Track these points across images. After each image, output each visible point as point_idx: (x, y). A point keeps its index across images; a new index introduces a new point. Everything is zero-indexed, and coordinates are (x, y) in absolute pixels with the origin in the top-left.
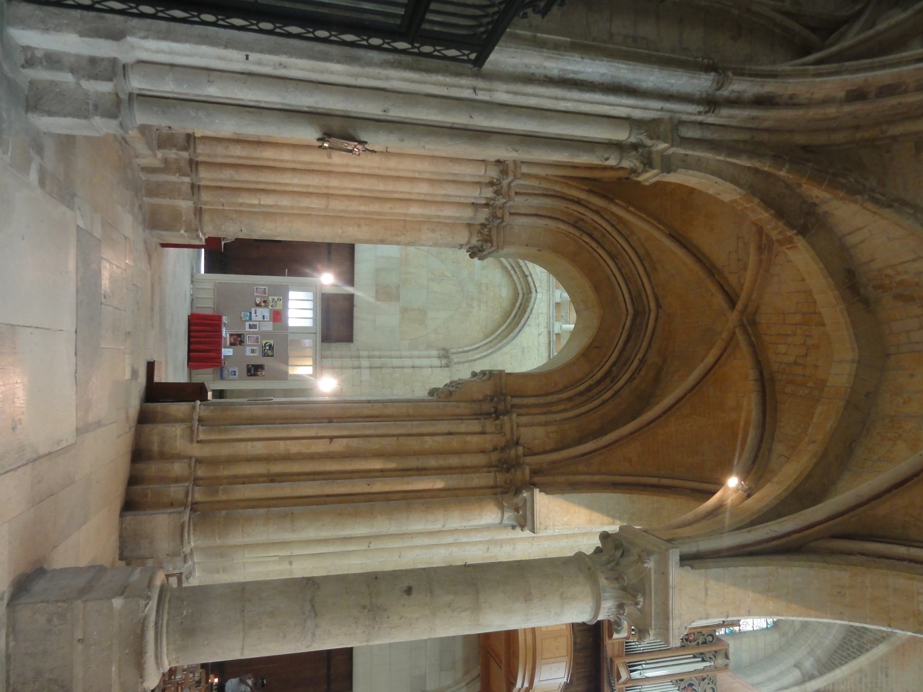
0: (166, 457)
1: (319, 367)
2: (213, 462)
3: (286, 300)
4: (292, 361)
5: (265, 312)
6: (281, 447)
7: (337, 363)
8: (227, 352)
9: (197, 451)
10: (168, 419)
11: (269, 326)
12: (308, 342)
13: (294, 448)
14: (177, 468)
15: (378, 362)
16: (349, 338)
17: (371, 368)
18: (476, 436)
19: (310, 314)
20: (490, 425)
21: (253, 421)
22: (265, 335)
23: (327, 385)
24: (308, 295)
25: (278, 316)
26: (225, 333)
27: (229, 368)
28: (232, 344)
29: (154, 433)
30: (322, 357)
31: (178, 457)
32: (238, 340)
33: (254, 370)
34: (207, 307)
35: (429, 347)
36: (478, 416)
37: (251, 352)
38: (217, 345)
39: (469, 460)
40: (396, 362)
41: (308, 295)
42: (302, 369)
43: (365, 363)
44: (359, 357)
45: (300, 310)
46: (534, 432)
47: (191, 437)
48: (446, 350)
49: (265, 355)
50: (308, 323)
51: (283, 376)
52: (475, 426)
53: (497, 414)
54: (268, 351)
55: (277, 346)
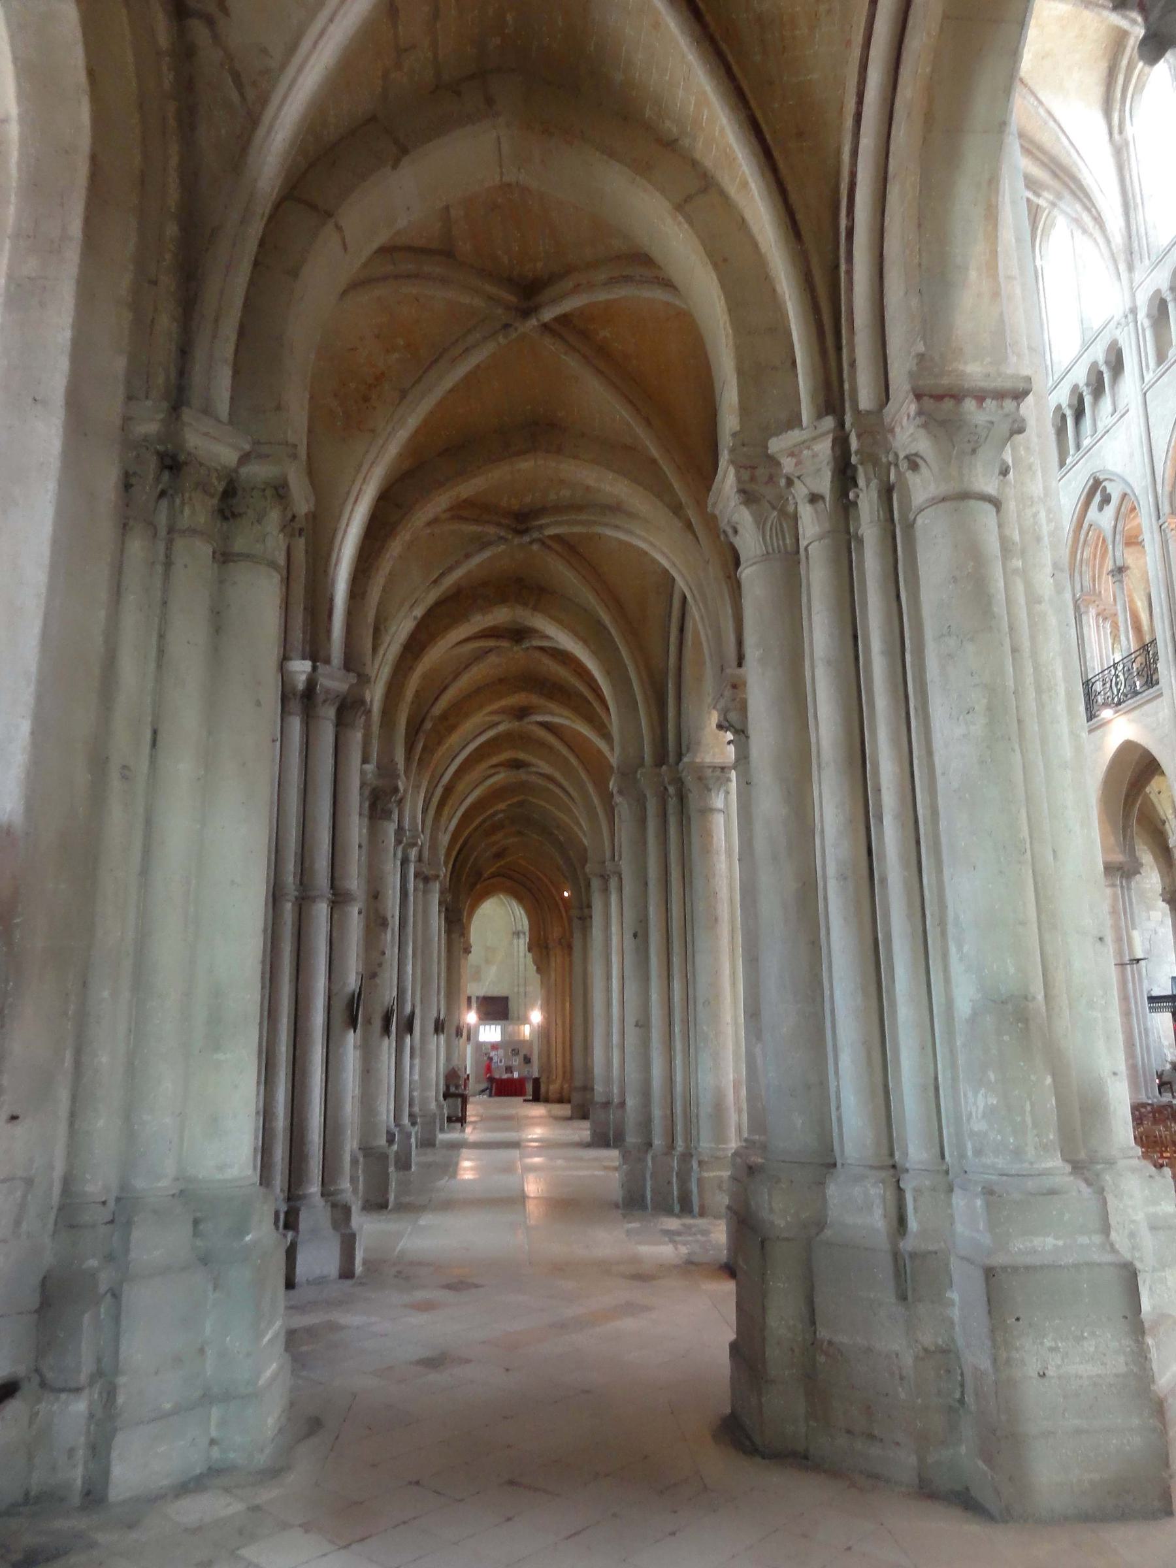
1: (525, 1020)
2: (564, 1073)
3: (484, 1043)
4: (522, 1038)
6: (560, 1046)
8: (516, 1075)
9: (559, 1081)
10: (547, 1092)
11: (501, 1052)
12: (510, 1028)
13: (560, 1040)
14: (566, 1086)
17: (525, 985)
18: (557, 960)
19: (493, 1027)
21: (549, 1056)
22: (506, 1054)
23: (536, 1016)
24: (482, 1028)
25: (495, 1046)
26: (505, 1076)
27: (525, 1074)
29: (552, 1095)
30: (519, 1019)
31: (562, 1088)
32: (509, 1069)
33: (527, 1060)
35: (511, 944)
37: (516, 1062)
38: (511, 1081)
40: (522, 968)
41: (482, 1028)
42: (526, 1031)
45: (491, 1034)
46: (556, 933)
49: (518, 1054)
50: (499, 1028)
51: (531, 1043)
52: (553, 959)
54: (515, 1052)
55: (512, 1046)
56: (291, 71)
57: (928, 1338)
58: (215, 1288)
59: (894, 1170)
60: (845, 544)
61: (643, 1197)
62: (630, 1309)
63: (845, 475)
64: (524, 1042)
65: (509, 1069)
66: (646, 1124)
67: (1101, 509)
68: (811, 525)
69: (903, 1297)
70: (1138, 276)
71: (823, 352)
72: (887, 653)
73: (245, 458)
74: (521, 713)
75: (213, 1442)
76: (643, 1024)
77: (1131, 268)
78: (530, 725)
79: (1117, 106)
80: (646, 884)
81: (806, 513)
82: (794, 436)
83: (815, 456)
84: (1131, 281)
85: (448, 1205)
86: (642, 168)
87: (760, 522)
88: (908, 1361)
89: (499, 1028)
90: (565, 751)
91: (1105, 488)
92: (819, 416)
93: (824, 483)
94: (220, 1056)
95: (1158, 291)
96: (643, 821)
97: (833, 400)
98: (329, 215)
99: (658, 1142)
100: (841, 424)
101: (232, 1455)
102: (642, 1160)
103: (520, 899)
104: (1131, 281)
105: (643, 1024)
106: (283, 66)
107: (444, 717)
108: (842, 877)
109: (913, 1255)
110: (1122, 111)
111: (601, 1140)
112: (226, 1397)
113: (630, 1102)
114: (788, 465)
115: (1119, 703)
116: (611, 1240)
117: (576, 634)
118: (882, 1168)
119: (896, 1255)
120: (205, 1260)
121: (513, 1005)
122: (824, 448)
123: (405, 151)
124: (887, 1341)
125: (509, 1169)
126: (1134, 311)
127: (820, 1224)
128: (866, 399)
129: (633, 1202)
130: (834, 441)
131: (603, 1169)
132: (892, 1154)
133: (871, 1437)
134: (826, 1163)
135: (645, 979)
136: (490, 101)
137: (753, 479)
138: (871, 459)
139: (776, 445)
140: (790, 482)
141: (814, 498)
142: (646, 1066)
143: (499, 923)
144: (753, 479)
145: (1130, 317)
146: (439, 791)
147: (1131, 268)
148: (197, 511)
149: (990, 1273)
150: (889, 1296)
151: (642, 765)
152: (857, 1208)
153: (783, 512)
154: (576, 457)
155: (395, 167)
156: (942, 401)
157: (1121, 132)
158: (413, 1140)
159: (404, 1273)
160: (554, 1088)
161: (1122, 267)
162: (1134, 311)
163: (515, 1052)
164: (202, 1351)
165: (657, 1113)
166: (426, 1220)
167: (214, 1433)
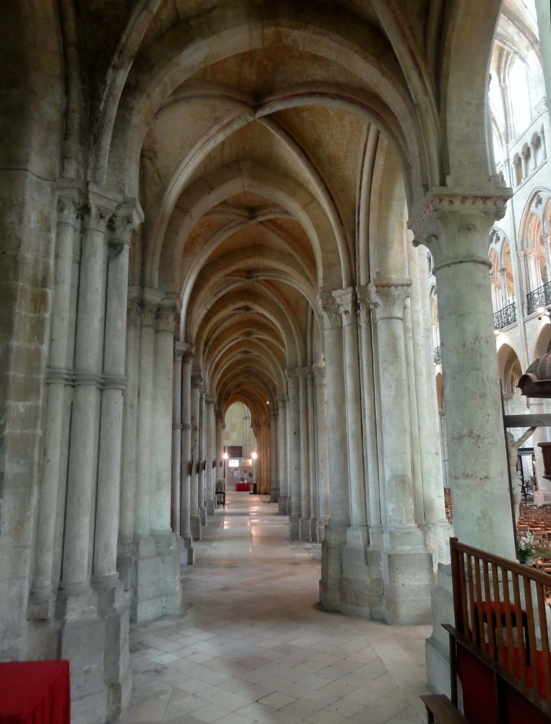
0: (266, 489)
1: (249, 457)
2: (267, 481)
3: (231, 468)
5: (236, 473)
6: (265, 469)
7: (248, 451)
8: (246, 482)
11: (239, 471)
12: (243, 461)
13: (265, 466)
15: (248, 439)
16: (240, 448)
17: (249, 441)
19: (235, 460)
20: (262, 428)
21: (260, 474)
22: (241, 473)
23: (255, 456)
24: (230, 461)
25: (236, 469)
26: (241, 482)
28: (244, 481)
29: (262, 491)
30: (247, 457)
32: (243, 479)
33: (251, 475)
34: (234, 487)
35: (243, 423)
36: (260, 429)
37: (246, 476)
38: (244, 484)
39: (268, 433)
40: (248, 433)
41: (230, 461)
42: (250, 462)
43: (248, 443)
44: (246, 445)
45: (234, 463)
46: (263, 418)
47: (263, 485)
48: (244, 418)
50: (238, 461)
51: (252, 467)
53: (260, 426)
54: (245, 471)
55: (244, 469)
56: (177, 174)
57: (374, 576)
58: (163, 562)
59: (366, 526)
60: (356, 326)
61: (298, 535)
62: (291, 574)
63: (356, 306)
64: (249, 467)
65: (243, 479)
66: (299, 508)
67: (496, 243)
68: (346, 321)
69: (367, 564)
70: (510, 145)
71: (350, 262)
72: (368, 365)
73: (163, 299)
74: (249, 334)
75: (164, 607)
76: (298, 469)
77: (507, 142)
78: (253, 337)
79: (503, 70)
80: (299, 413)
81: (344, 316)
82: (340, 292)
83: (346, 299)
84: (507, 147)
85: (221, 539)
86: (292, 194)
87: (330, 317)
88: (368, 583)
89: (238, 461)
90: (266, 348)
91: (497, 234)
92: (348, 286)
93: (349, 308)
94: (161, 492)
95: (517, 154)
96: (297, 388)
97: (353, 282)
98: (188, 212)
99: (304, 514)
100: (355, 290)
101: (169, 611)
102: (297, 521)
103: (246, 404)
104: (507, 147)
105: (298, 469)
106: (174, 172)
107: (217, 339)
108: (353, 436)
109: (371, 552)
110: (505, 72)
111: (284, 512)
112: (167, 595)
113: (294, 500)
114: (338, 301)
115: (502, 327)
116: (285, 551)
117: (271, 313)
118: (363, 526)
119: (366, 552)
120: (159, 554)
121: (244, 450)
122: (349, 297)
123: (212, 189)
124: (363, 576)
125: (245, 524)
126: (508, 160)
127: (345, 543)
128: (363, 281)
129: (295, 537)
130: (352, 295)
131: (282, 524)
132: (367, 522)
133: (357, 605)
134: (347, 524)
135: (299, 450)
136: (240, 170)
137: (327, 303)
138: (364, 301)
139: (335, 294)
140: (339, 306)
141: (346, 312)
142: (299, 485)
143: (238, 414)
144: (327, 303)
145: (507, 163)
146: (214, 365)
147: (507, 142)
148: (149, 319)
149: (389, 556)
150: (363, 564)
151: (297, 366)
152: (355, 538)
153: (337, 314)
154: (270, 258)
155: (209, 194)
156: (384, 288)
157: (504, 82)
158: (206, 513)
159: (210, 563)
160: (263, 489)
161: (504, 141)
162: (508, 160)
163: (245, 471)
164: (159, 581)
165: (303, 503)
166: (215, 544)
167: (164, 605)
